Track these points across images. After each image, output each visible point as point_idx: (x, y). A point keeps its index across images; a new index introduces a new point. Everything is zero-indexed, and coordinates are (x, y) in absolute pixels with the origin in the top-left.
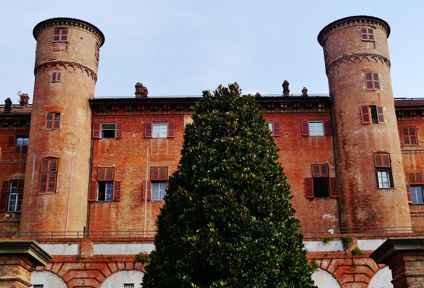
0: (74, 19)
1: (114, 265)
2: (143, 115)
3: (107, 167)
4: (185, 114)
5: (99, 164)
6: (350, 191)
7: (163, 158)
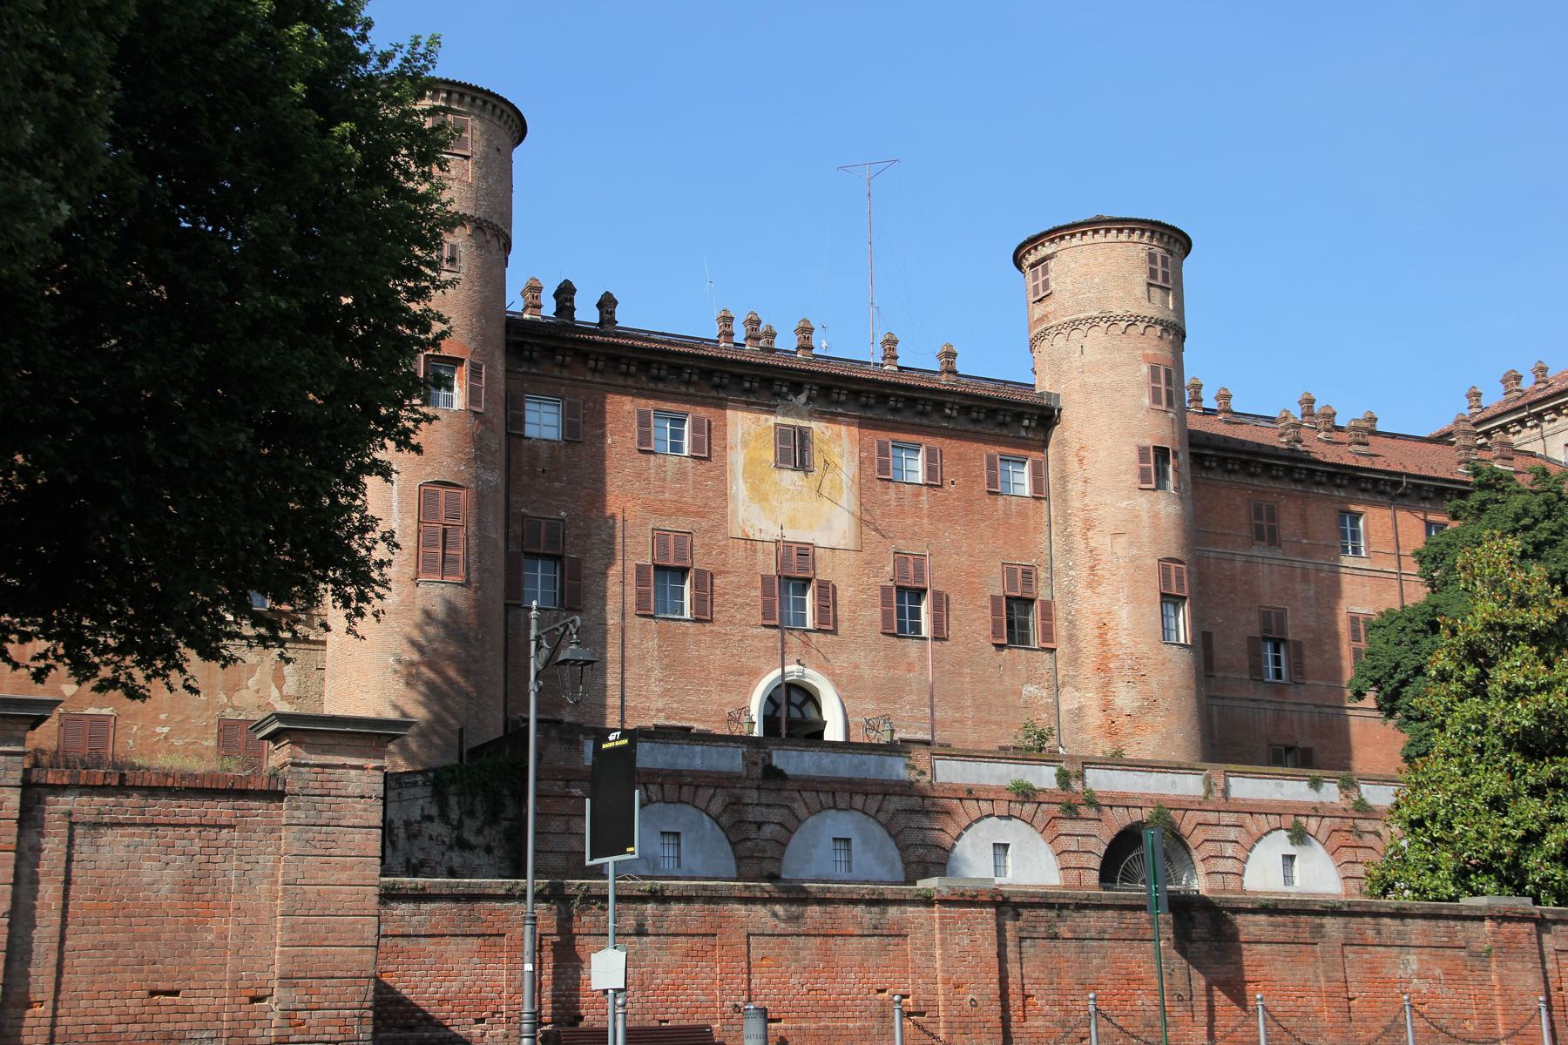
0: (488, 93)
1: (975, 802)
2: (632, 388)
3: (546, 516)
4: (732, 401)
5: (526, 507)
6: (1097, 640)
7: (681, 510)
